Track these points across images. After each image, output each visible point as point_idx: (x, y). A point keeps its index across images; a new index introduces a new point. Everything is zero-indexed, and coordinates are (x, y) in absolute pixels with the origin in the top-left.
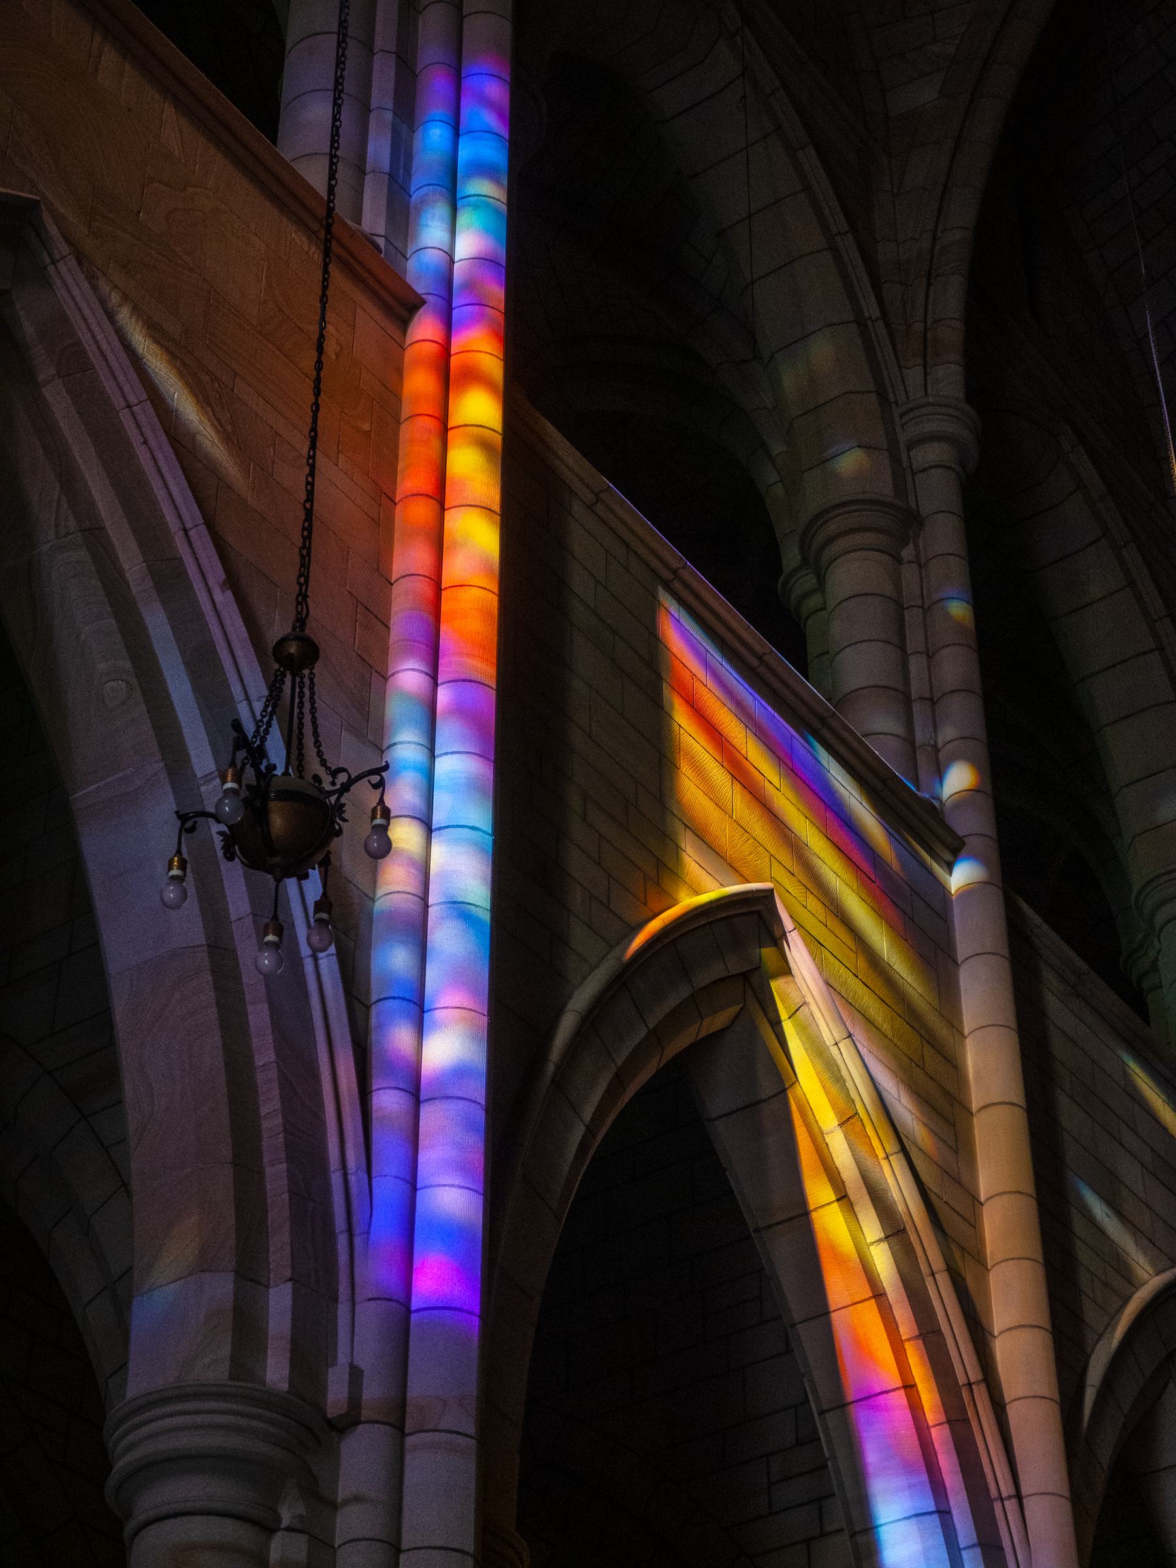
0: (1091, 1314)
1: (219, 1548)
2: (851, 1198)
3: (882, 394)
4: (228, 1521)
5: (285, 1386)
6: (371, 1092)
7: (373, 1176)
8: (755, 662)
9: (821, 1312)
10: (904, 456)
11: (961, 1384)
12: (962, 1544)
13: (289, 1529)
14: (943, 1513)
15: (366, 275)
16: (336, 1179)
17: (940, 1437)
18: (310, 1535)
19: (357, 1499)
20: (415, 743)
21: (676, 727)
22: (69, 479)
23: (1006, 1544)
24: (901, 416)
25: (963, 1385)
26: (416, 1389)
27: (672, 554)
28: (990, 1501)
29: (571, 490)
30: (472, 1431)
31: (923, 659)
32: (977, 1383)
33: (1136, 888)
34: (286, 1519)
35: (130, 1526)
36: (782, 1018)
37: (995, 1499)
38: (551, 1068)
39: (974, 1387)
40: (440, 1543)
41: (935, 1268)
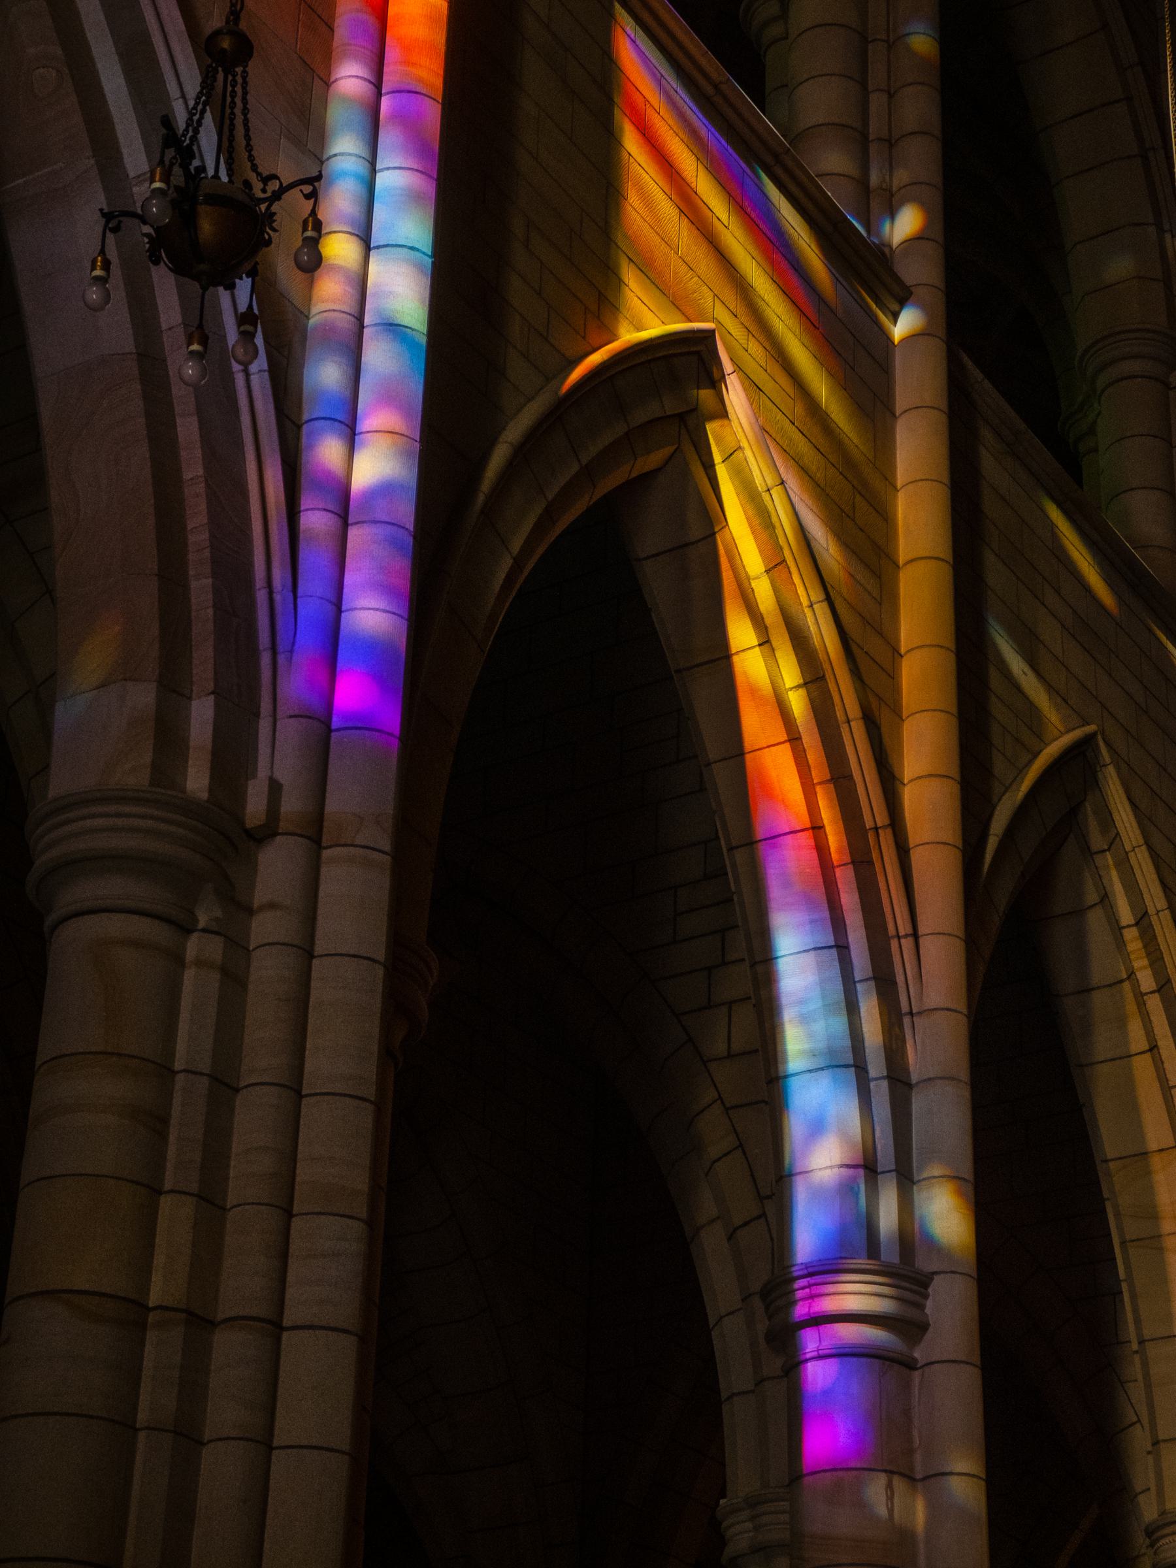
0: (999, 766)
5: (205, 796)
6: (300, 512)
7: (299, 595)
8: (709, 90)
9: (736, 751)
11: (868, 828)
12: (857, 977)
13: (204, 930)
14: (841, 948)
16: (261, 596)
17: (845, 879)
18: (225, 936)
19: (272, 906)
20: (356, 155)
21: (625, 156)
23: (900, 979)
25: (870, 829)
26: (333, 805)
28: (888, 939)
30: (387, 848)
32: (884, 827)
34: (203, 920)
35: (49, 921)
36: (716, 462)
37: (893, 937)
38: (481, 498)
39: (880, 831)
40: (352, 952)
41: (851, 716)
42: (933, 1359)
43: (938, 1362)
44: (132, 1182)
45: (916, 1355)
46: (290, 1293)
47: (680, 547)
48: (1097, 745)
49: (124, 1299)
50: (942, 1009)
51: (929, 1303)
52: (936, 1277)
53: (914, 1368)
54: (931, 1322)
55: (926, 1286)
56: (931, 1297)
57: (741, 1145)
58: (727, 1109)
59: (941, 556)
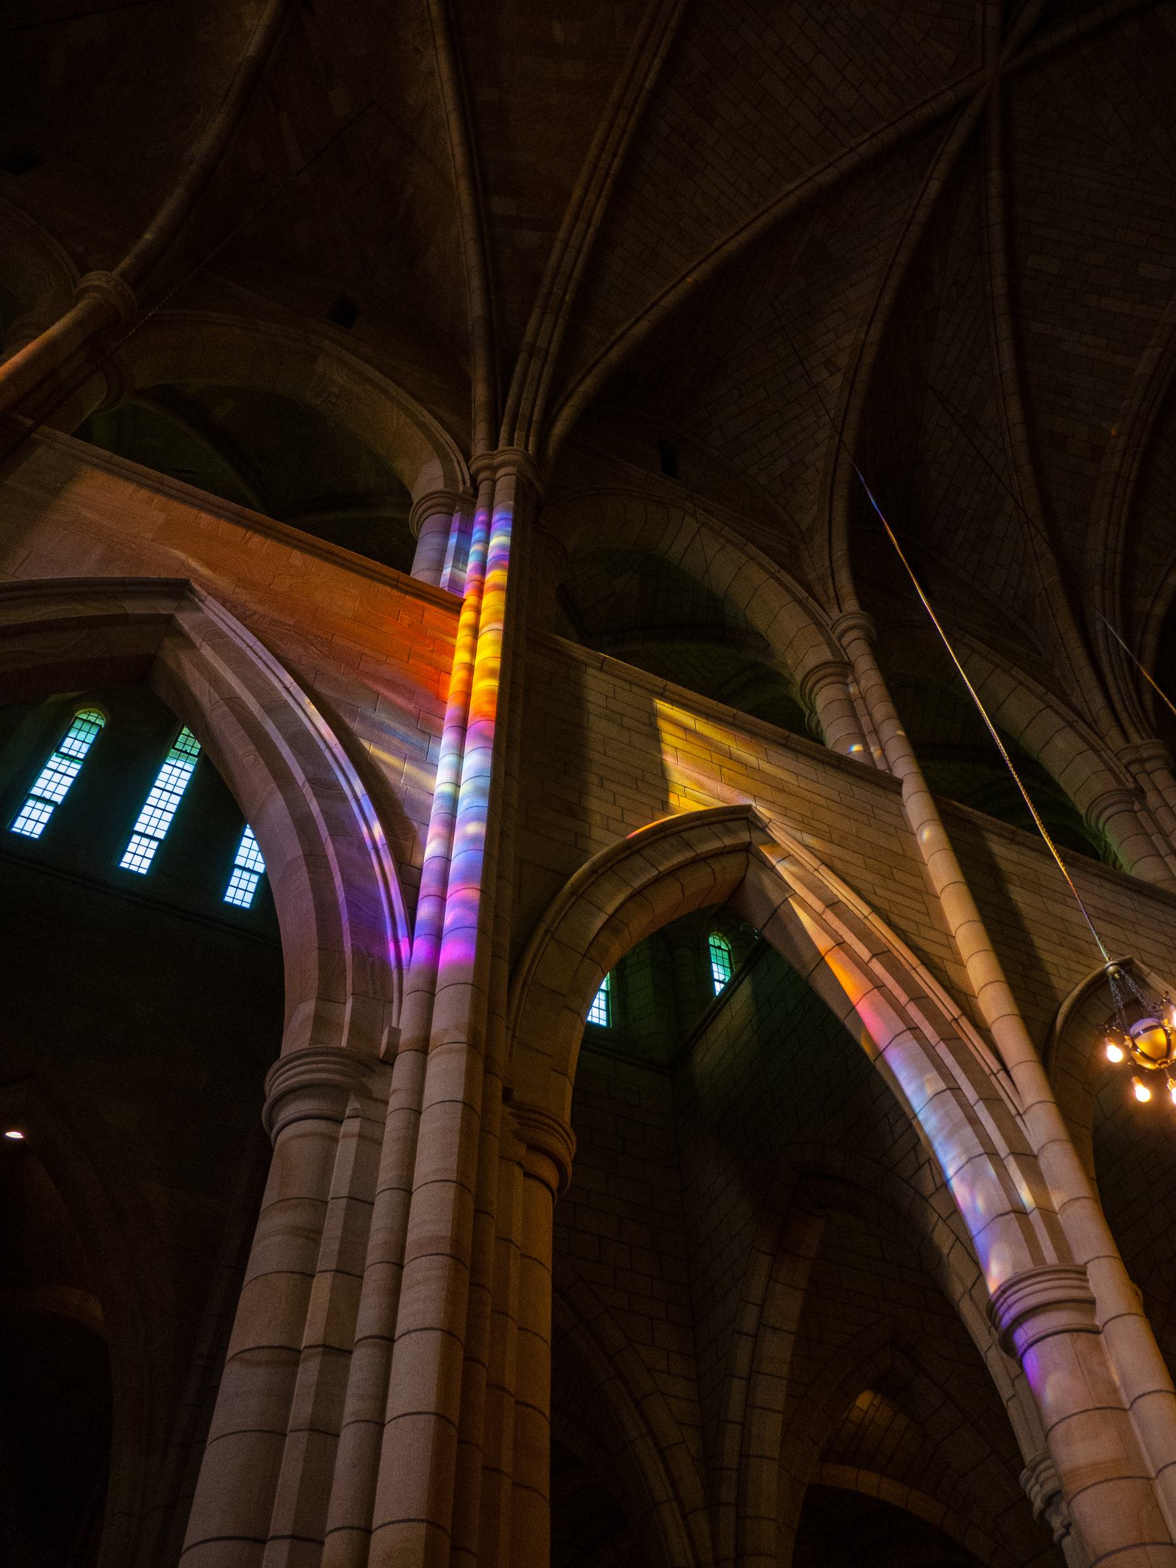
2: (848, 942)
3: (818, 624)
10: (837, 642)
13: (349, 1117)
14: (955, 1089)
15: (428, 596)
22: (215, 681)
24: (831, 629)
26: (434, 1030)
27: (659, 681)
29: (586, 665)
30: (464, 1039)
31: (867, 717)
37: (990, 1075)
39: (959, 1020)
41: (915, 966)
43: (1109, 1320)
47: (774, 913)
48: (1137, 964)
49: (277, 1347)
50: (1036, 1103)
51: (1091, 1284)
55: (1084, 1273)
56: (1090, 1280)
57: (958, 1239)
58: (945, 1221)
59: (956, 880)
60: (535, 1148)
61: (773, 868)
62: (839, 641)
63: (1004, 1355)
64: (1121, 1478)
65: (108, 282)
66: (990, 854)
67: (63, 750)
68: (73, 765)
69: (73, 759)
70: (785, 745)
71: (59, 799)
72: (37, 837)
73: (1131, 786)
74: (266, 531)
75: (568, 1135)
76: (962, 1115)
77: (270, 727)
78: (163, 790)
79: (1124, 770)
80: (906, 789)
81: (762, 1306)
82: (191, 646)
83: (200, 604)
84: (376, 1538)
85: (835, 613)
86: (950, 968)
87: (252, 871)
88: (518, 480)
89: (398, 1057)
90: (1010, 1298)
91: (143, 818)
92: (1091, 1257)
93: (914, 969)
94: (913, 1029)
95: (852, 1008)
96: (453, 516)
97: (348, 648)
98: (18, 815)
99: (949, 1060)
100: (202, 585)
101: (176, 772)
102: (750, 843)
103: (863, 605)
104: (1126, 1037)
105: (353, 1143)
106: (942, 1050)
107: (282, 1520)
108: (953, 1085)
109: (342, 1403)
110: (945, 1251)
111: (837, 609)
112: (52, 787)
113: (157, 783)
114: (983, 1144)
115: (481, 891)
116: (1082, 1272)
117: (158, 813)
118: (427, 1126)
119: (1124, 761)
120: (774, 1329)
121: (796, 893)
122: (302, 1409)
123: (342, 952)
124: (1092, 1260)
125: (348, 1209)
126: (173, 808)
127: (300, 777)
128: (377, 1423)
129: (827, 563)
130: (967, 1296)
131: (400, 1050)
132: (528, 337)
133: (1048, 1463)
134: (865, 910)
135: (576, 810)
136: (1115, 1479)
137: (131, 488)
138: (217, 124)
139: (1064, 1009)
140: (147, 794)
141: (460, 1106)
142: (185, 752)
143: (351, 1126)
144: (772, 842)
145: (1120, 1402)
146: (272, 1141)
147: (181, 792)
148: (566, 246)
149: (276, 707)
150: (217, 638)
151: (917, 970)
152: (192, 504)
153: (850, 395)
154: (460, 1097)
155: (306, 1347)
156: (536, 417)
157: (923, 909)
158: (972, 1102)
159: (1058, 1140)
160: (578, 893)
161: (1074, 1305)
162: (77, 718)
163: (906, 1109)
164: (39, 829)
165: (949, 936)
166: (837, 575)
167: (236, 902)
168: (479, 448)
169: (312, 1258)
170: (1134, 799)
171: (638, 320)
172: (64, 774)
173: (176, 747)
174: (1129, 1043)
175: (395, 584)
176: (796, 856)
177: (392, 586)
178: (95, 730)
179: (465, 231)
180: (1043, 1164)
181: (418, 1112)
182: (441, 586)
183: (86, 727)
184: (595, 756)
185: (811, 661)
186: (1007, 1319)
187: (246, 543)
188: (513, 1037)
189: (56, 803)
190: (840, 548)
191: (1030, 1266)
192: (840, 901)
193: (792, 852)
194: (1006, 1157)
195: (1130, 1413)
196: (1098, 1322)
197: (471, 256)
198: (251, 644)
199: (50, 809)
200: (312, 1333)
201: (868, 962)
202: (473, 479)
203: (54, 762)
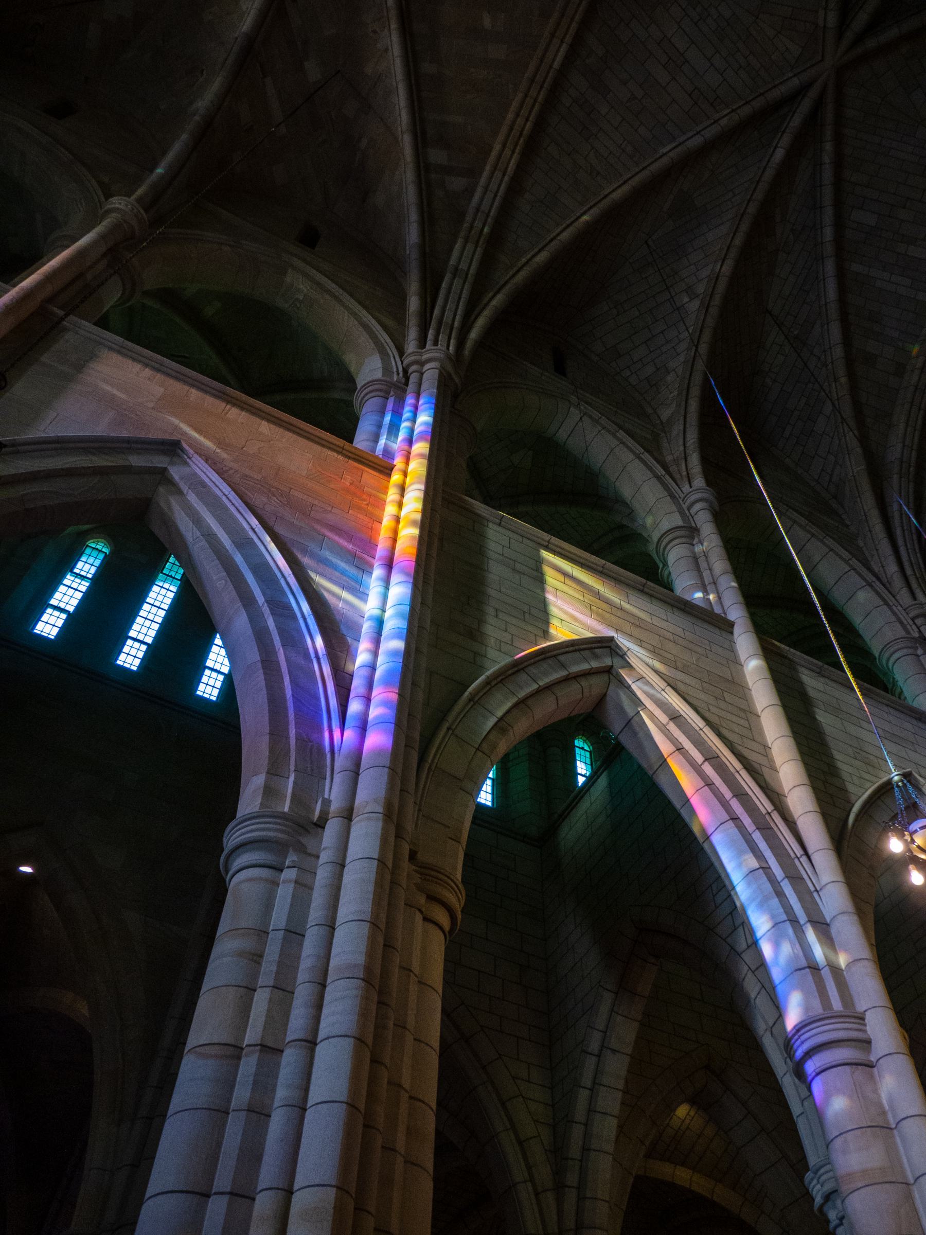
1: (250, 880)
3: (672, 496)
4: (255, 869)
10: (687, 512)
13: (288, 867)
22: (197, 521)
23: (805, 876)
26: (357, 802)
27: (546, 536)
30: (381, 810)
31: (708, 571)
32: (772, 811)
33: (877, 657)
39: (772, 814)
41: (738, 770)
42: (879, 1057)
44: (236, 986)
45: (872, 1059)
46: (323, 1024)
47: (628, 723)
48: (915, 777)
50: (829, 883)
51: (868, 1028)
52: (868, 1014)
53: (872, 1067)
54: (872, 1038)
55: (863, 1019)
57: (763, 986)
58: (753, 972)
60: (432, 898)
61: (629, 687)
62: (689, 510)
63: (797, 1080)
64: (886, 1182)
65: (127, 205)
66: (801, 683)
67: (76, 571)
68: (83, 583)
69: (83, 578)
70: (642, 591)
71: (71, 609)
72: (53, 637)
73: (916, 635)
74: (242, 406)
75: (457, 887)
76: (772, 889)
77: (238, 559)
78: (153, 605)
79: (911, 623)
80: (737, 630)
81: (605, 1032)
82: (180, 492)
83: (188, 460)
84: (297, 1198)
85: (686, 488)
86: (766, 772)
87: (219, 672)
88: (441, 374)
89: (328, 822)
90: (803, 1036)
91: (135, 627)
92: (870, 1006)
93: (738, 772)
94: (735, 819)
95: (687, 800)
96: (388, 399)
97: (302, 499)
98: (39, 620)
99: (763, 845)
100: (190, 445)
101: (163, 591)
102: (612, 666)
103: (708, 483)
104: (906, 833)
105: (291, 887)
106: (757, 836)
107: (223, 1180)
108: (765, 865)
109: (274, 1090)
110: (753, 995)
111: (688, 486)
112: (66, 599)
113: (148, 600)
114: (786, 913)
115: (399, 694)
116: (861, 1018)
117: (148, 623)
118: (349, 877)
119: (912, 614)
120: (614, 1051)
121: (646, 707)
122: (242, 1094)
123: (288, 737)
124: (870, 1009)
125: (284, 939)
126: (160, 620)
127: (260, 599)
128: (301, 1108)
129: (682, 448)
130: (768, 1033)
131: (331, 815)
132: (453, 262)
133: (828, 1167)
134: (701, 723)
135: (475, 634)
136: (881, 1183)
137: (138, 367)
138: (216, 85)
139: (856, 809)
140: (140, 608)
141: (376, 862)
142: (171, 576)
143: (289, 874)
144: (629, 666)
145: (888, 1122)
146: (227, 883)
147: (166, 607)
148: (486, 189)
149: (245, 544)
150: (200, 487)
151: (740, 772)
152: (185, 382)
153: (706, 315)
154: (376, 855)
155: (247, 1046)
156: (456, 324)
157: (747, 726)
158: (779, 879)
159: (846, 912)
160: (475, 700)
161: (853, 1043)
162: (88, 546)
163: (727, 883)
164: (55, 631)
165: (766, 747)
166: (689, 459)
167: (206, 696)
168: (411, 346)
169: (255, 975)
170: (918, 645)
171: (539, 251)
172: (76, 590)
173: (164, 572)
174: (908, 838)
175: (341, 451)
176: (648, 678)
177: (338, 452)
178: (101, 556)
179: (407, 176)
180: (834, 931)
181: (343, 866)
182: (377, 454)
183: (95, 553)
184: (491, 592)
185: (665, 525)
186: (799, 1053)
187: (226, 414)
188: (419, 810)
189: (69, 612)
190: (692, 437)
191: (820, 1011)
192: (681, 715)
193: (645, 675)
194: (805, 923)
195: (895, 1131)
196: (873, 1058)
197: (411, 194)
198: (227, 493)
199: (64, 616)
200: (252, 1035)
201: (701, 765)
202: (405, 371)
203: (68, 579)
